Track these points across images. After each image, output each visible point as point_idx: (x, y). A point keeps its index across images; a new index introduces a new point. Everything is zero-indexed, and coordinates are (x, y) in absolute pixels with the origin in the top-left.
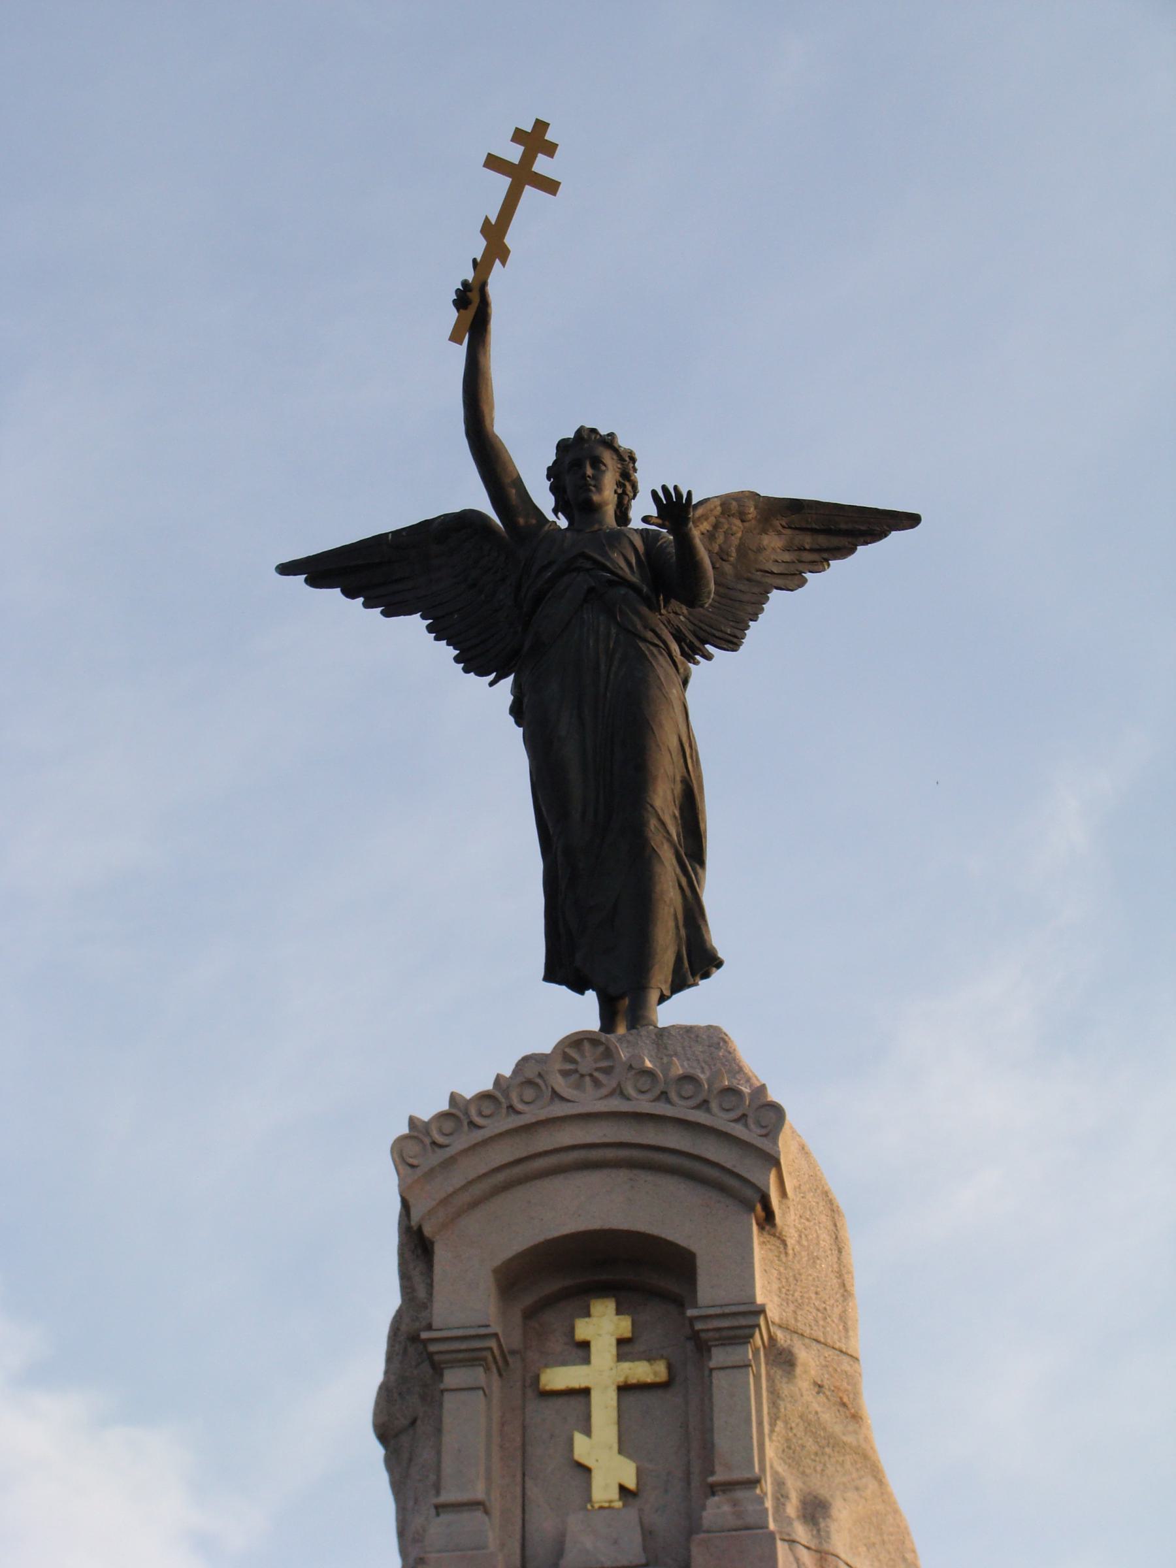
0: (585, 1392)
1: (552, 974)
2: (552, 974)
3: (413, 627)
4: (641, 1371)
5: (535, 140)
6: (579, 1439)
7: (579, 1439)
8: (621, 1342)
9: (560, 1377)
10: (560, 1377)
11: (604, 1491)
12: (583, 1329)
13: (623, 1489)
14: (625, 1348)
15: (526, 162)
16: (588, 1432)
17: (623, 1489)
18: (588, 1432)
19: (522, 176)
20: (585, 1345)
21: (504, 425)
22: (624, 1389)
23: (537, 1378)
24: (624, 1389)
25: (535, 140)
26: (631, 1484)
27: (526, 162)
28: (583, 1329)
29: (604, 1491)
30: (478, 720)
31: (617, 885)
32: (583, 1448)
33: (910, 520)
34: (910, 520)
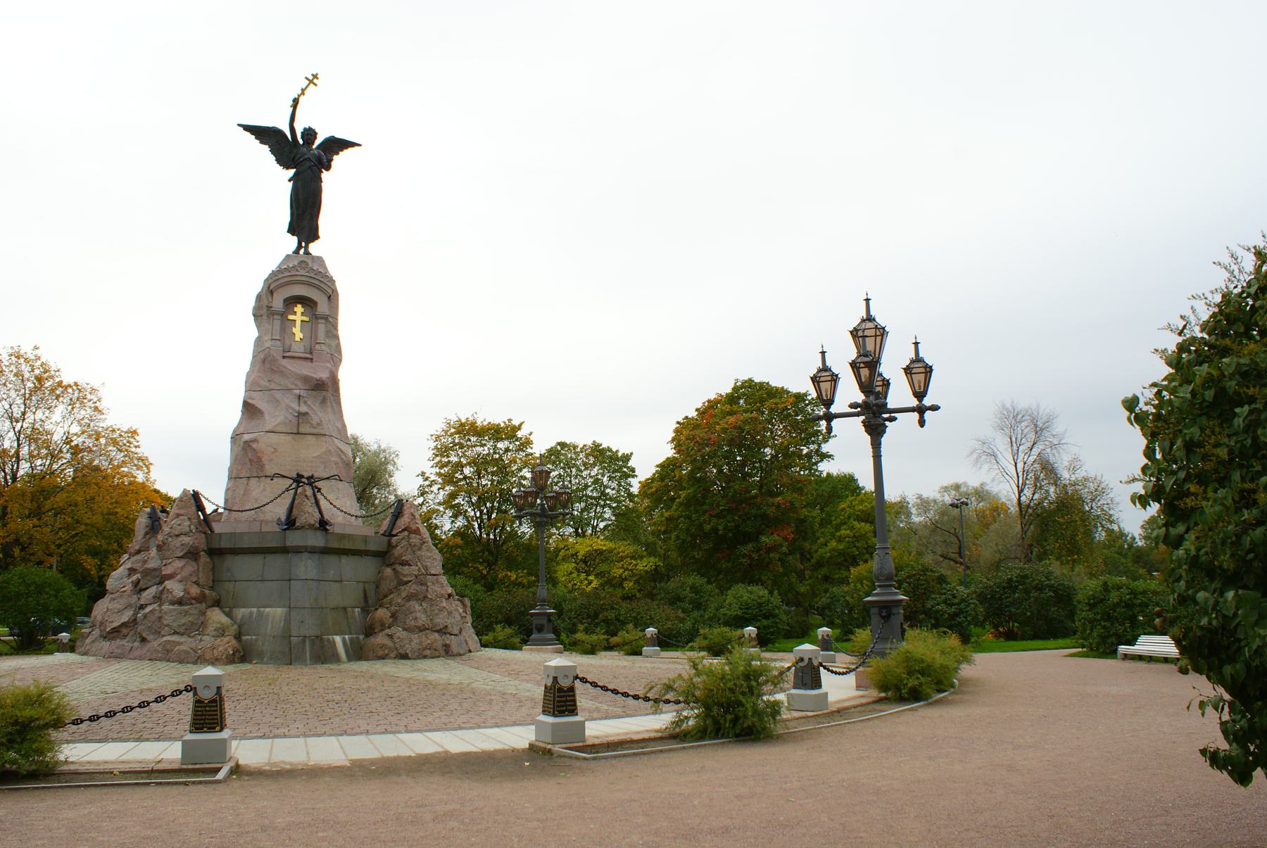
1: (289, 231)
2: (289, 231)
3: (266, 148)
4: (305, 319)
5: (315, 76)
9: (291, 317)
10: (291, 317)
11: (297, 339)
15: (313, 80)
19: (311, 82)
21: (295, 125)
25: (315, 76)
27: (313, 80)
29: (297, 339)
30: (281, 181)
31: (304, 218)
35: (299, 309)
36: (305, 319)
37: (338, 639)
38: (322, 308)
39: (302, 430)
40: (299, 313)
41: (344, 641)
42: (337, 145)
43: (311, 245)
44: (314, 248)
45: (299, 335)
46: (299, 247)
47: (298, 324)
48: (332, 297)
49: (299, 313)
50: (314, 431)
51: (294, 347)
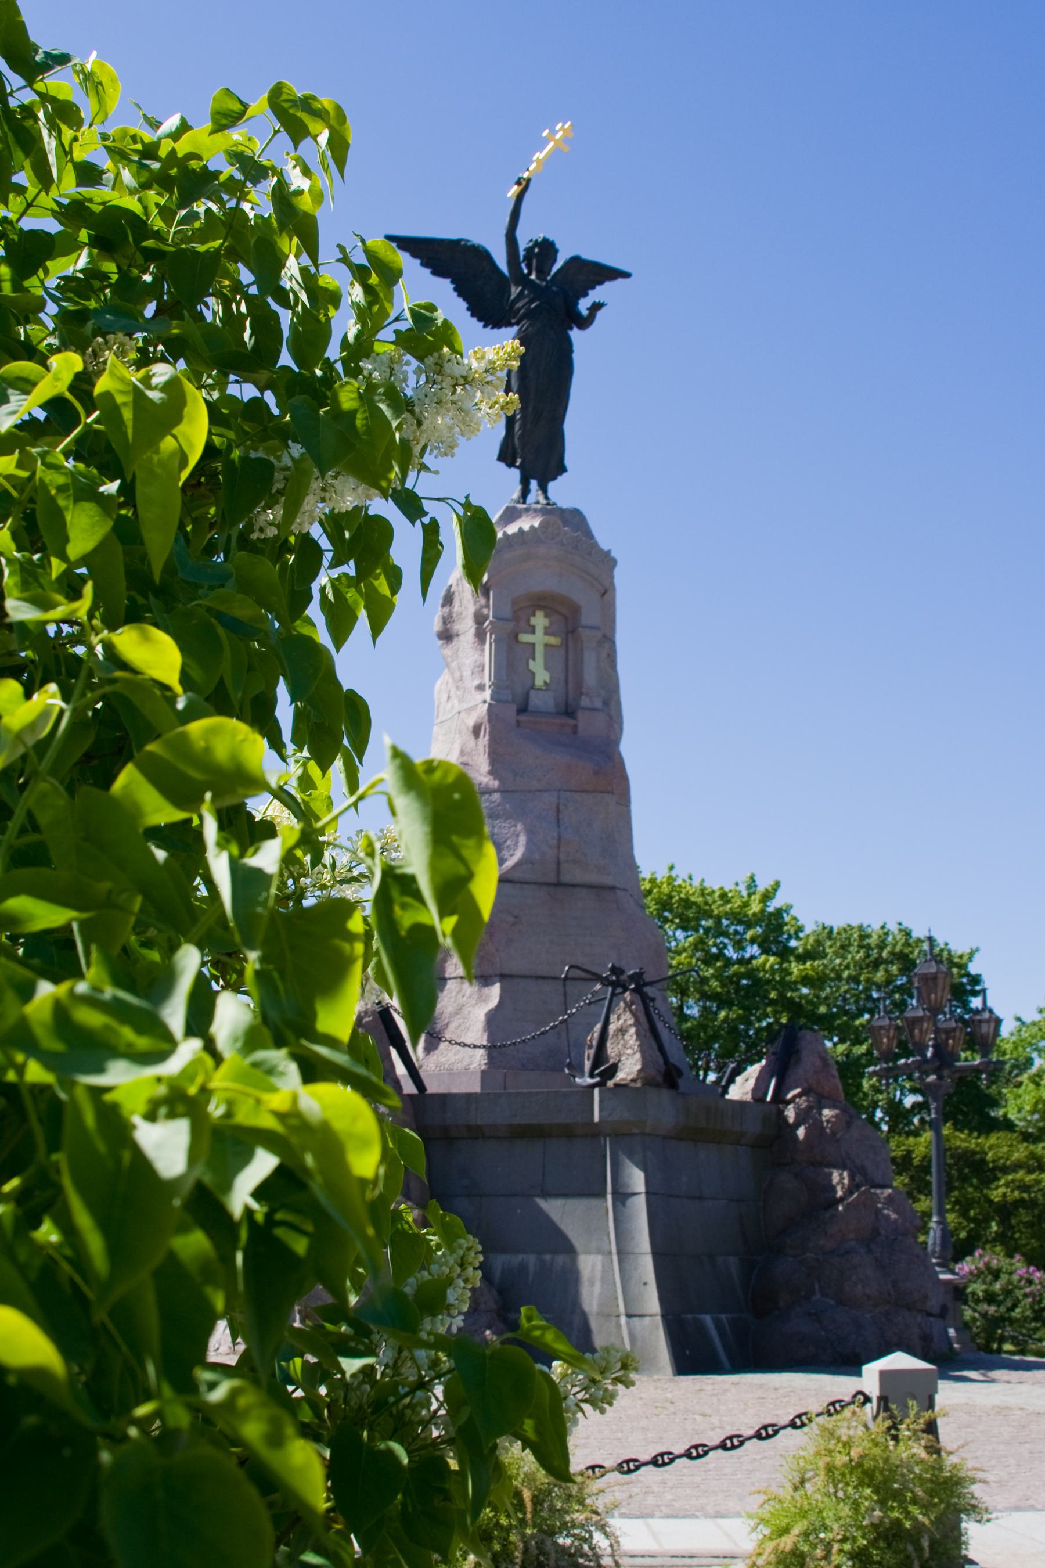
0: (534, 645)
1: (501, 458)
2: (501, 458)
4: (553, 640)
6: (531, 662)
7: (531, 662)
8: (545, 628)
9: (525, 638)
10: (525, 638)
12: (533, 621)
13: (545, 682)
14: (547, 632)
16: (534, 659)
17: (545, 682)
18: (534, 659)
20: (534, 627)
22: (546, 645)
23: (516, 636)
24: (546, 645)
26: (548, 681)
28: (533, 621)
29: (539, 682)
32: (532, 665)
33: (626, 275)
34: (626, 275)
35: (540, 621)
36: (553, 640)
37: (708, 1319)
38: (589, 617)
39: (566, 878)
40: (540, 631)
41: (718, 1324)
42: (594, 273)
43: (552, 486)
44: (562, 492)
45: (542, 677)
46: (525, 492)
47: (539, 651)
48: (606, 592)
49: (540, 631)
50: (592, 878)
51: (537, 701)
